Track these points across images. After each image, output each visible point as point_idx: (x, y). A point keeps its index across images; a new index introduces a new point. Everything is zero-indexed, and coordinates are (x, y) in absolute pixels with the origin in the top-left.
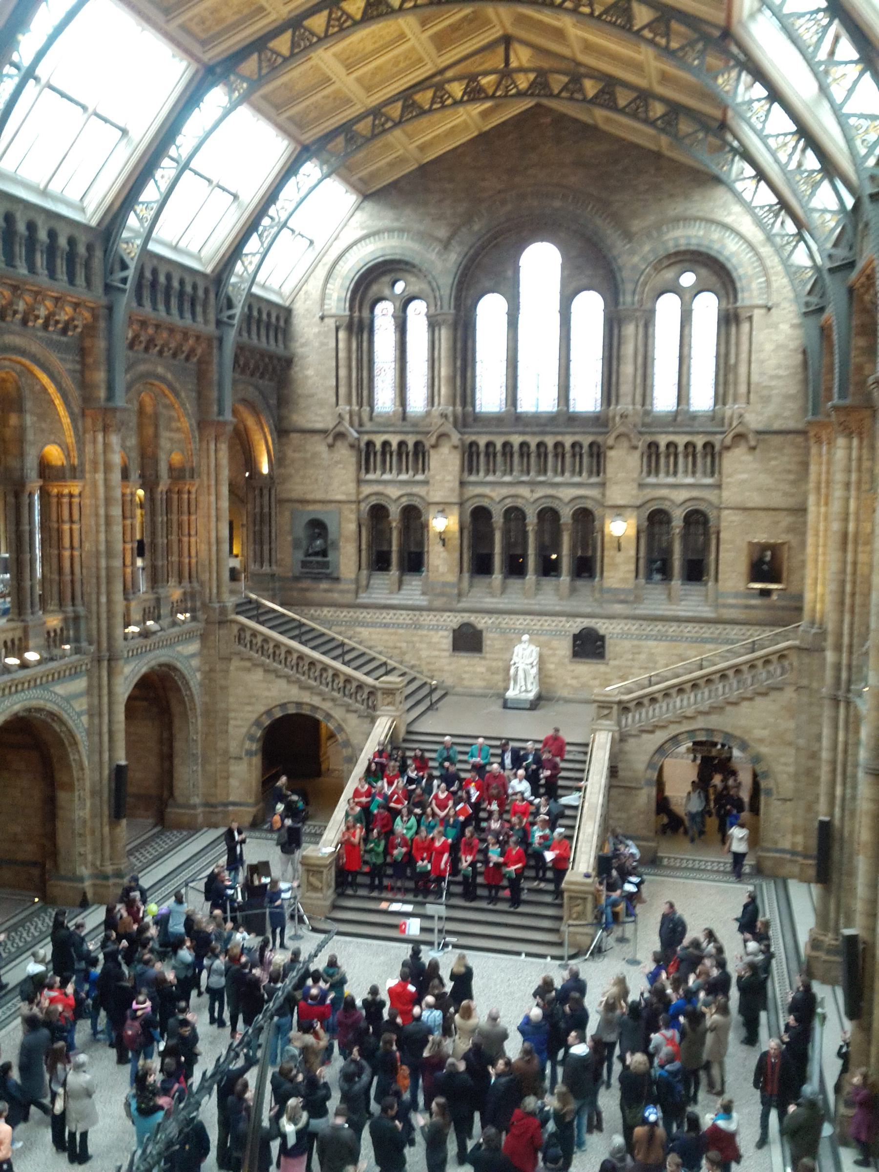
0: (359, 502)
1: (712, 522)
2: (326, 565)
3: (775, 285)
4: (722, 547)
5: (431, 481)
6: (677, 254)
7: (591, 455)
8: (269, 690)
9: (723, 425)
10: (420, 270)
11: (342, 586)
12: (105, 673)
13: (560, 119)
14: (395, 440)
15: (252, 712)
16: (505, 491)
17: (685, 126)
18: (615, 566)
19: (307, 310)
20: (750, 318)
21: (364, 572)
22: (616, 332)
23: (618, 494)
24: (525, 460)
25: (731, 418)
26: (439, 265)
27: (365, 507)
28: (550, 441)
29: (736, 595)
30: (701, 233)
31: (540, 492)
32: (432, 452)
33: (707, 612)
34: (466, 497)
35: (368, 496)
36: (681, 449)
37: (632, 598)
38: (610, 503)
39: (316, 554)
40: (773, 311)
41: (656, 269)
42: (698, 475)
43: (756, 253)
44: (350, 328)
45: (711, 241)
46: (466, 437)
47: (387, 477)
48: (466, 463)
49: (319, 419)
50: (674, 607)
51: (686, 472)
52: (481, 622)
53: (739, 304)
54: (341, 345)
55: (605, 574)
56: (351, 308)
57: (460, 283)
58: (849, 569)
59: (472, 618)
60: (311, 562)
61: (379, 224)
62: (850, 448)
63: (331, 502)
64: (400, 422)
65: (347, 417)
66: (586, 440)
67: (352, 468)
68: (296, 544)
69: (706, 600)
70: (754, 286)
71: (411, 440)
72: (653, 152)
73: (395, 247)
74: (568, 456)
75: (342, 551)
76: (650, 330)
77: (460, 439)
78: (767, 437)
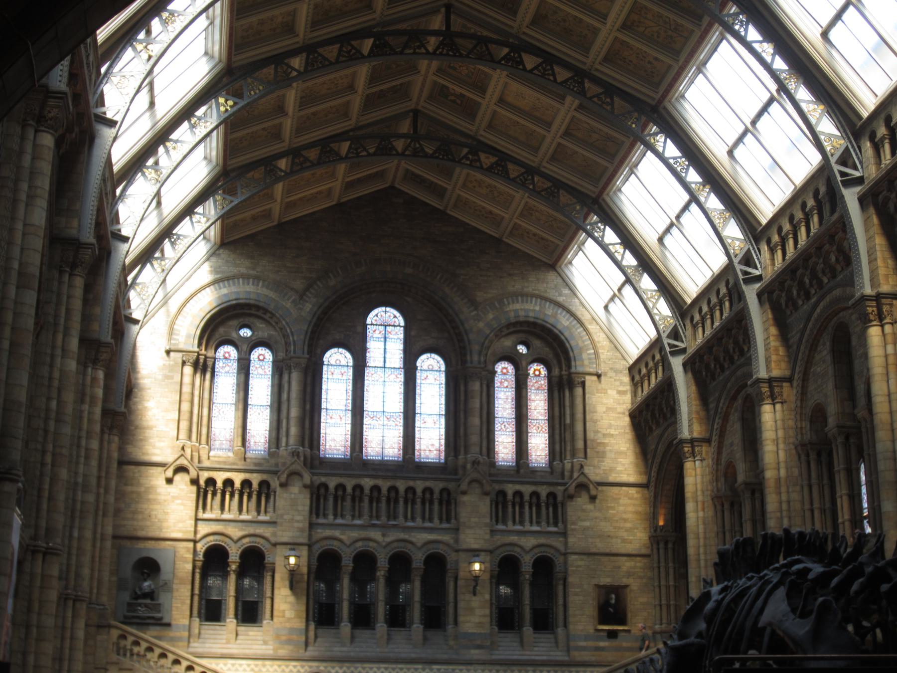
1: (559, 568)
2: (157, 607)
3: (602, 357)
4: (571, 590)
6: (515, 324)
7: (441, 503)
9: (563, 479)
10: (273, 315)
12: (69, 614)
16: (355, 534)
17: (564, 198)
18: (471, 610)
20: (583, 384)
21: (196, 621)
22: (462, 388)
23: (472, 538)
24: (374, 504)
25: (572, 471)
27: (201, 547)
28: (401, 486)
29: (587, 638)
30: (537, 308)
31: (393, 536)
32: (278, 489)
33: (560, 656)
34: (314, 538)
36: (527, 498)
37: (489, 644)
38: (464, 546)
40: (603, 378)
41: (496, 336)
42: (544, 524)
44: (196, 365)
45: (546, 314)
46: (315, 478)
48: (314, 505)
50: (528, 653)
51: (531, 522)
53: (573, 370)
55: (461, 619)
56: (200, 345)
57: (313, 332)
58: (784, 506)
60: (140, 605)
61: (235, 271)
64: (243, 462)
66: (437, 486)
68: (121, 585)
69: (557, 646)
71: (255, 479)
72: (491, 236)
73: (249, 293)
74: (419, 501)
75: (175, 594)
76: (492, 389)
77: (311, 479)
78: (604, 488)
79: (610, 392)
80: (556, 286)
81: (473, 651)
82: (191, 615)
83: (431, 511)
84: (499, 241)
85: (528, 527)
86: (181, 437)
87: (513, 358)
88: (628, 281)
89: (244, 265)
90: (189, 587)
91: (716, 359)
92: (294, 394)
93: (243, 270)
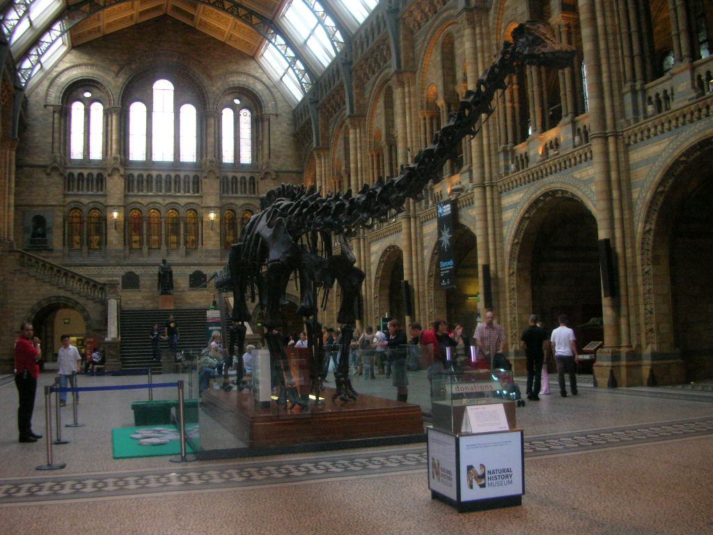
0: (64, 206)
2: (45, 242)
5: (108, 194)
6: (232, 88)
8: (39, 290)
10: (102, 85)
11: (54, 255)
13: (177, 22)
14: (86, 173)
15: (28, 304)
19: (37, 102)
26: (112, 82)
30: (245, 80)
35: (69, 203)
39: (39, 235)
41: (222, 94)
43: (271, 91)
47: (80, 193)
49: (42, 159)
51: (242, 193)
52: (138, 271)
54: (56, 121)
56: (62, 102)
57: (124, 93)
59: (133, 269)
60: (36, 240)
62: (356, 134)
63: (47, 206)
65: (59, 159)
67: (61, 187)
70: (270, 105)
71: (95, 172)
78: (279, 174)
79: (283, 124)
80: (255, 67)
81: (212, 259)
82: (64, 245)
83: (189, 188)
84: (223, 44)
85: (239, 195)
86: (54, 151)
87: (233, 107)
88: (290, 66)
89: (85, 59)
90: (62, 230)
91: (332, 106)
92: (114, 127)
93: (85, 61)
